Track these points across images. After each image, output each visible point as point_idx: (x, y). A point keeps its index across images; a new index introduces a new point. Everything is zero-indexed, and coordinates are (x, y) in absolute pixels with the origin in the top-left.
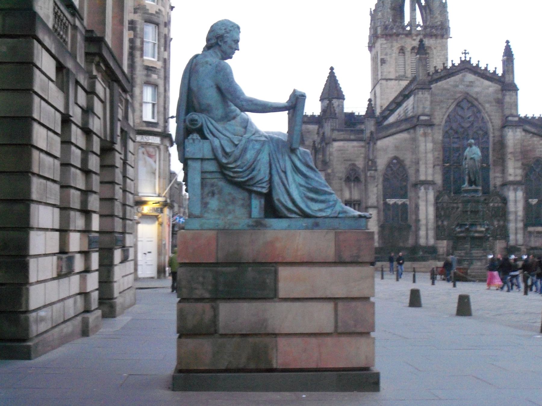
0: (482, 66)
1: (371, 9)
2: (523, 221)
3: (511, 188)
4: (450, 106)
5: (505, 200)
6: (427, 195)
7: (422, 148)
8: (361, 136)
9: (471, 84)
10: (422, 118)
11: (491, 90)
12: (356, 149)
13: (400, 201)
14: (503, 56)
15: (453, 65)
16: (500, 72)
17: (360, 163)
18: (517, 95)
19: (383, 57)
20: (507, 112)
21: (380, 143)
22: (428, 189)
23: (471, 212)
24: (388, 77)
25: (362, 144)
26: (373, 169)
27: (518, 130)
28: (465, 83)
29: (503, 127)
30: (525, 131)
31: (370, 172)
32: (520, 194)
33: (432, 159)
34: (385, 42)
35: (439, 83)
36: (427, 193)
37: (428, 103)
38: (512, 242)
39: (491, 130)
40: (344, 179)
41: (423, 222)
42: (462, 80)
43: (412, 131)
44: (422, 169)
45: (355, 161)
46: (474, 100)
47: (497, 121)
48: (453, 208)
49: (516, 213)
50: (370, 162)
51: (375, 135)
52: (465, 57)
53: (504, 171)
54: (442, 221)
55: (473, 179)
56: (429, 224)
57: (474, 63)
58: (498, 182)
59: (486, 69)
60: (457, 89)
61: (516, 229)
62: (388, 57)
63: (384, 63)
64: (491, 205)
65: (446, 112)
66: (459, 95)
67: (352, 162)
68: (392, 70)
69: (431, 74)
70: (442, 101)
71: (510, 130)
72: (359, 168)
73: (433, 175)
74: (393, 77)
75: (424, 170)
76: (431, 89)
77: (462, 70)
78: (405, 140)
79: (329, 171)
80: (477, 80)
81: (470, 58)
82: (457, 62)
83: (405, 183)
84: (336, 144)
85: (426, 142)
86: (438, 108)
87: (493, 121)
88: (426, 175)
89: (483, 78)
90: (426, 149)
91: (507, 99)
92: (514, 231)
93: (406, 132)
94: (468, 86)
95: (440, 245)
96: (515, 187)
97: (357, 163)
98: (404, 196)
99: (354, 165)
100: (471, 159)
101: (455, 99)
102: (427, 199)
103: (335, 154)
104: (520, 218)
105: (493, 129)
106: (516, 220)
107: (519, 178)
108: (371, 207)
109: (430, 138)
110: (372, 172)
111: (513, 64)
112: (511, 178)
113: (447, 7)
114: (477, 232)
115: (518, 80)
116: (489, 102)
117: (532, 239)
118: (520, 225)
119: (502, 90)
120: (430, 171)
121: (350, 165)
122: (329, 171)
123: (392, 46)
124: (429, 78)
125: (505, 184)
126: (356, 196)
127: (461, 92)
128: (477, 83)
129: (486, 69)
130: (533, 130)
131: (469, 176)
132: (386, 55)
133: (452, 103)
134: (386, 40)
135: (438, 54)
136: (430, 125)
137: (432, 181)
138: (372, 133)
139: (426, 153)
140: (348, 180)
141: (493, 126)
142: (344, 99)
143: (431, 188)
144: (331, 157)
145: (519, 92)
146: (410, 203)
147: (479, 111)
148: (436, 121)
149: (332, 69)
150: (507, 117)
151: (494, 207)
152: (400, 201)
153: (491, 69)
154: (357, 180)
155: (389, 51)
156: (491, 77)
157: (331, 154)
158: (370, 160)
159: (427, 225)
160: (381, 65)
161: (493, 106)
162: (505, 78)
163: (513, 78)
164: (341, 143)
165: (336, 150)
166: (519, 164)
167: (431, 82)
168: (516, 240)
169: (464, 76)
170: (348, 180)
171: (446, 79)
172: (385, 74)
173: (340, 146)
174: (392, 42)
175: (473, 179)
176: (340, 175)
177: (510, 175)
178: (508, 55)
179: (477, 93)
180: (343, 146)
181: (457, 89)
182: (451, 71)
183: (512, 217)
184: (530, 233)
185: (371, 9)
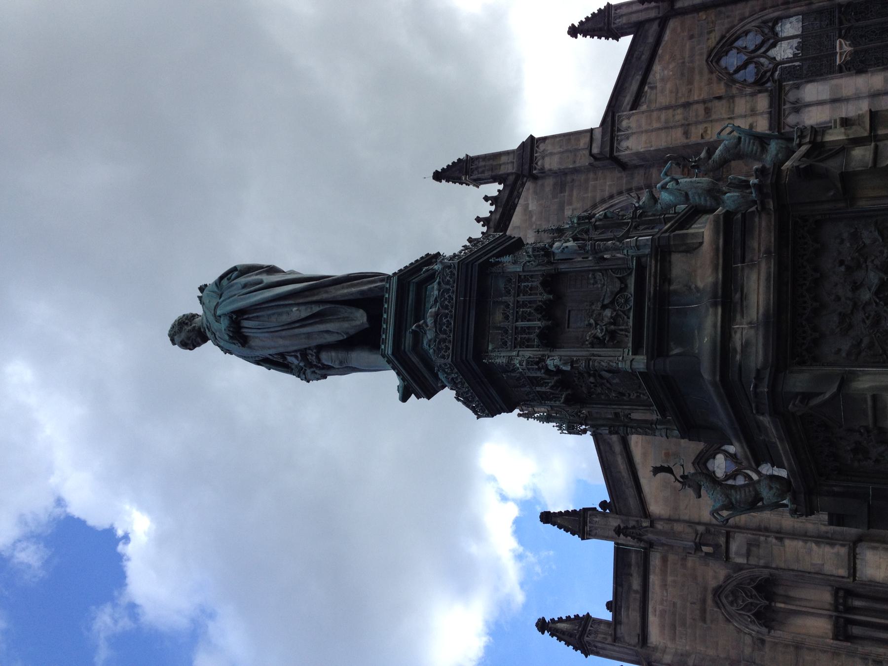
3: (792, 119)
8: (633, 558)
11: (533, 206)
12: (670, 579)
16: (493, 189)
17: (715, 574)
18: (544, 139)
20: (584, 160)
21: (656, 508)
23: (550, 339)
25: (655, 560)
26: (722, 541)
29: (623, 166)
30: (635, 105)
31: (732, 555)
40: (764, 630)
45: (705, 589)
47: (607, 183)
50: (705, 549)
55: (360, 318)
59: (486, 221)
67: (710, 601)
71: (624, 144)
72: (728, 577)
84: (655, 635)
87: (607, 194)
91: (551, 163)
97: (713, 584)
99: (717, 592)
107: (763, 102)
108: (853, 570)
110: (734, 547)
111: (478, 158)
116: (561, 208)
119: (535, 178)
121: (718, 604)
126: (826, 597)
129: (486, 221)
130: (634, 87)
140: (766, 617)
141: (620, 193)
145: (537, 136)
153: (486, 209)
156: (504, 206)
161: (571, 195)
162: (508, 174)
163: (507, 153)
164: (653, 621)
165: (673, 639)
166: (720, 109)
170: (766, 617)
173: (662, 627)
175: (360, 318)
176: (748, 640)
178: (462, 171)
180: (663, 613)
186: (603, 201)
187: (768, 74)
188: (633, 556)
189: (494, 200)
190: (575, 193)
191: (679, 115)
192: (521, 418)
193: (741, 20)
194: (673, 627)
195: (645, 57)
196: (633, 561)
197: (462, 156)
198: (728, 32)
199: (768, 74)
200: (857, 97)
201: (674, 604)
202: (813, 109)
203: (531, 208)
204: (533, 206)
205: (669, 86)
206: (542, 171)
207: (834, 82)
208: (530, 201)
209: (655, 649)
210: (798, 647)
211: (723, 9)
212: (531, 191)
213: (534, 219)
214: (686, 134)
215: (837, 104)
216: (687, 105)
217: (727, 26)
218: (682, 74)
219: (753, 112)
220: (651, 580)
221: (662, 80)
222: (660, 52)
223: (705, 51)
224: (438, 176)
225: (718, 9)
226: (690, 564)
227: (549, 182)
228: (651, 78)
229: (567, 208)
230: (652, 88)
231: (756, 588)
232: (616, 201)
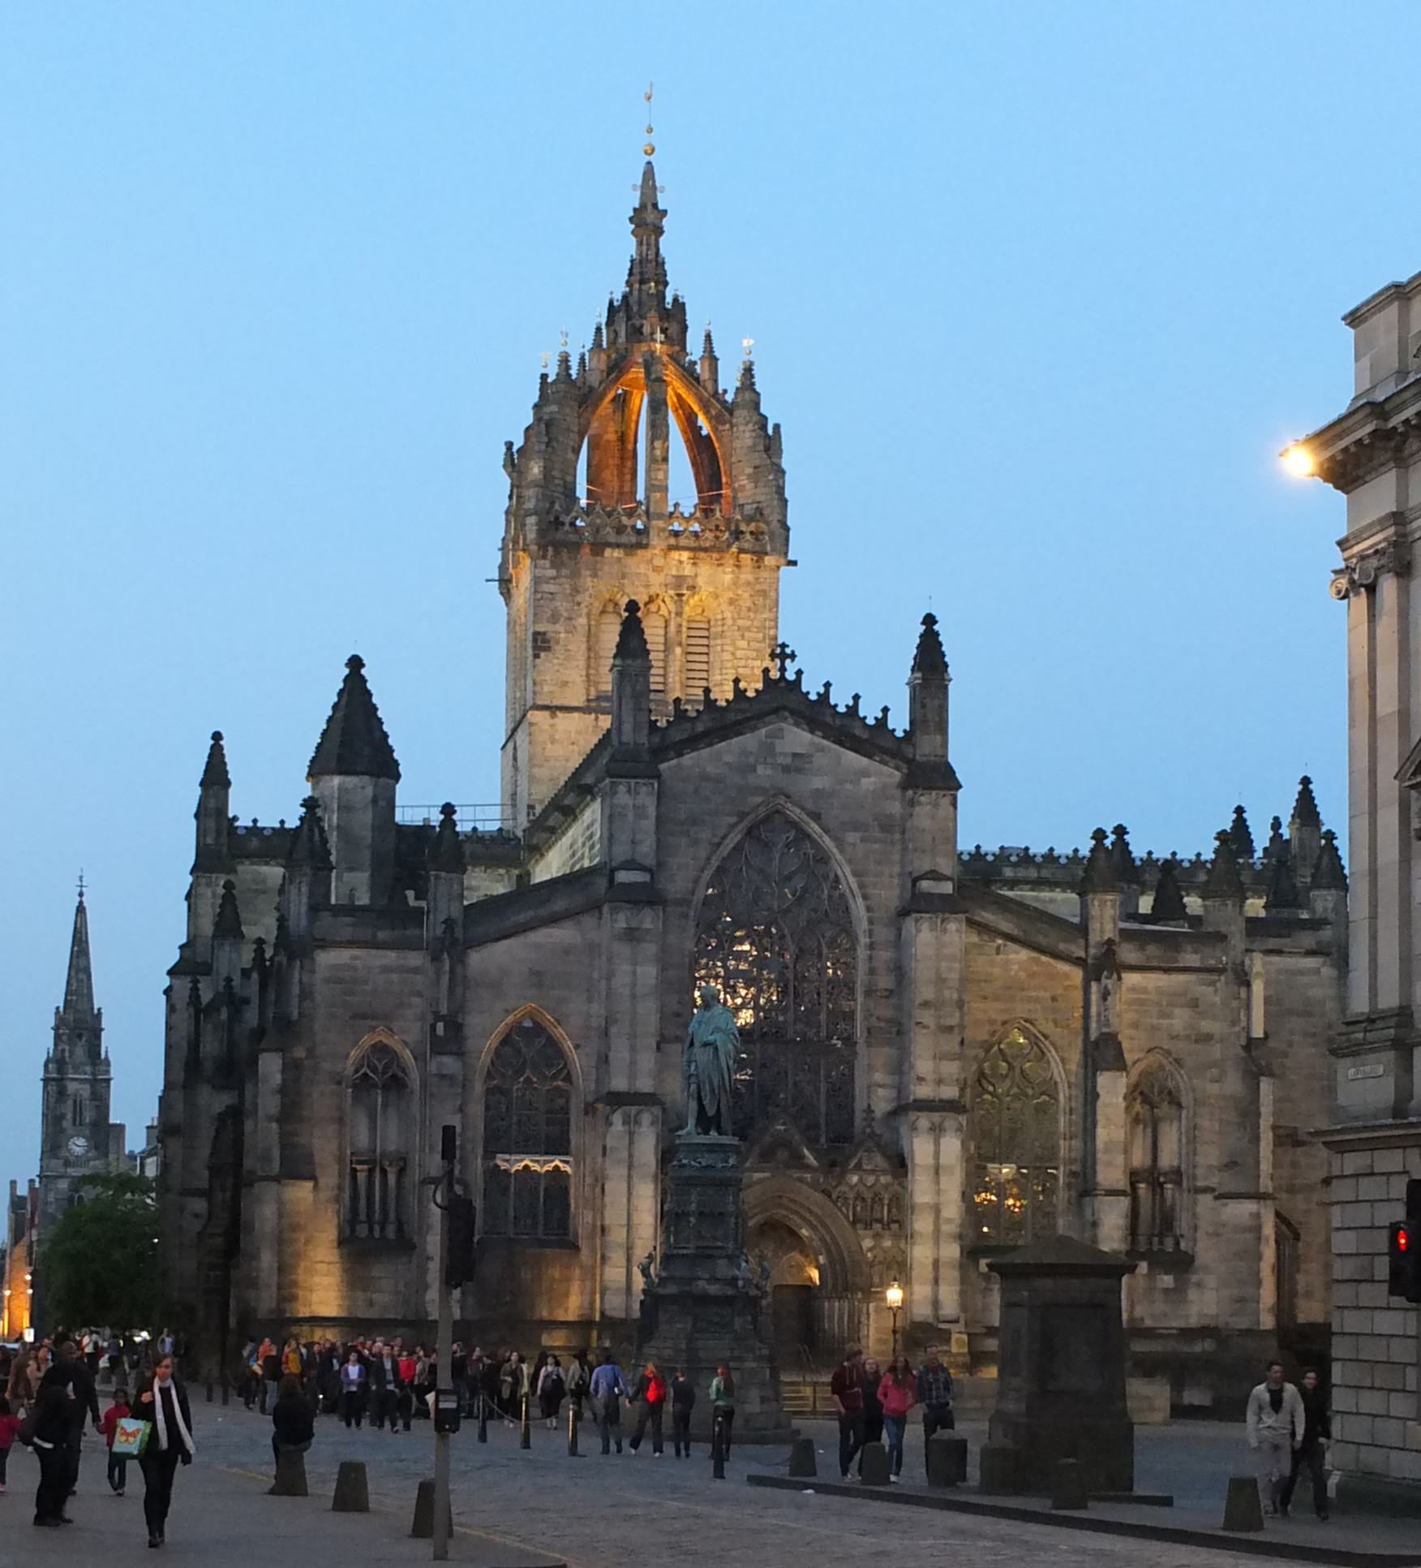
0: (840, 700)
1: (509, 445)
2: (961, 1237)
3: (924, 1121)
4: (724, 837)
5: (900, 1164)
6: (631, 1142)
7: (621, 982)
9: (799, 763)
10: (622, 877)
11: (867, 783)
12: (394, 977)
13: (540, 1165)
14: (913, 670)
15: (739, 693)
16: (899, 723)
18: (954, 805)
19: (541, 628)
21: (477, 959)
22: (637, 1123)
24: (556, 703)
25: (415, 959)
27: (952, 926)
28: (780, 760)
29: (904, 913)
32: (952, 1147)
33: (654, 1019)
34: (552, 572)
35: (688, 759)
36: (631, 1134)
37: (649, 824)
39: (865, 925)
41: (618, 1235)
42: (768, 750)
43: (588, 920)
44: (620, 1053)
46: (806, 818)
49: (937, 1210)
50: (440, 1026)
51: (459, 932)
52: (783, 669)
53: (900, 1068)
55: (711, 1112)
56: (639, 1243)
57: (812, 687)
58: (882, 1102)
61: (936, 1264)
62: (559, 627)
63: (548, 649)
64: (855, 1179)
65: (708, 859)
66: (759, 799)
68: (575, 674)
69: (662, 723)
70: (694, 821)
71: (925, 926)
73: (659, 1074)
74: (579, 701)
75: (626, 1055)
76: (658, 776)
77: (768, 714)
78: (567, 951)
79: (299, 1052)
80: (822, 749)
81: (799, 673)
82: (753, 686)
83: (561, 1101)
85: (635, 963)
86: (684, 841)
88: (632, 1076)
89: (841, 744)
90: (634, 985)
92: (928, 1273)
93: (569, 924)
94: (786, 769)
96: (936, 1117)
98: (558, 1145)
100: (706, 1044)
101: (742, 816)
102: (631, 1156)
103: (322, 991)
105: (871, 922)
107: (950, 1092)
109: (650, 949)
110: (447, 1060)
112: (923, 1091)
113: (779, 452)
114: (713, 1280)
115: (958, 757)
116: (856, 827)
118: (952, 1251)
119: (904, 786)
120: (647, 1060)
122: (299, 1052)
123: (576, 591)
124: (656, 739)
125: (903, 1108)
127: (758, 790)
128: (819, 760)
130: (1006, 926)
131: (700, 1099)
132: (554, 618)
133: (735, 825)
134: (553, 566)
135: (740, 622)
136: (648, 896)
137: (653, 1095)
138: (449, 923)
139: (633, 996)
140: (362, 1084)
141: (869, 909)
142: (397, 777)
144: (307, 1004)
145: (960, 793)
146: (577, 1165)
147: (823, 859)
148: (676, 884)
149: (355, 663)
150: (915, 881)
152: (540, 1165)
153: (869, 712)
154: (396, 1084)
155: (562, 606)
156: (872, 739)
157: (306, 994)
158: (438, 1017)
159: (629, 1249)
160: (536, 656)
163: (945, 744)
165: (328, 981)
166: (951, 1044)
167: (660, 752)
168: (936, 1303)
169: (778, 734)
171: (711, 745)
172: (546, 688)
173: (338, 967)
174: (575, 574)
175: (711, 1112)
177: (921, 1079)
179: (818, 794)
181: (751, 780)
182: (731, 717)
183: (922, 1224)
185: (509, 445)
186: (861, 886)
187: (991, 1088)
188: (417, 932)
189: (882, 722)
190: (876, 846)
191: (951, 995)
192: (504, 449)
193: (1063, 1060)
194: (340, 981)
195: (1041, 940)
196: (408, 933)
198: (1053, 1045)
199: (991, 1088)
200: (938, 1192)
201: (366, 983)
202: (932, 1147)
203: (864, 781)
204: (867, 783)
205: (997, 971)
206: (912, 803)
207: (958, 1169)
208: (877, 777)
209: (313, 960)
210: (341, 1120)
211: (1081, 1038)
212: (888, 780)
213: (849, 786)
214: (926, 1004)
215: (932, 1171)
216: (960, 1004)
217: (1059, 1043)
218: (1010, 988)
220: (389, 953)
221: (1007, 962)
222: (1044, 958)
223: (1033, 1016)
225: (1081, 1032)
226: (416, 1000)
227: (895, 808)
229: (858, 835)
230: (998, 949)
231: (394, 1076)
232: (860, 901)
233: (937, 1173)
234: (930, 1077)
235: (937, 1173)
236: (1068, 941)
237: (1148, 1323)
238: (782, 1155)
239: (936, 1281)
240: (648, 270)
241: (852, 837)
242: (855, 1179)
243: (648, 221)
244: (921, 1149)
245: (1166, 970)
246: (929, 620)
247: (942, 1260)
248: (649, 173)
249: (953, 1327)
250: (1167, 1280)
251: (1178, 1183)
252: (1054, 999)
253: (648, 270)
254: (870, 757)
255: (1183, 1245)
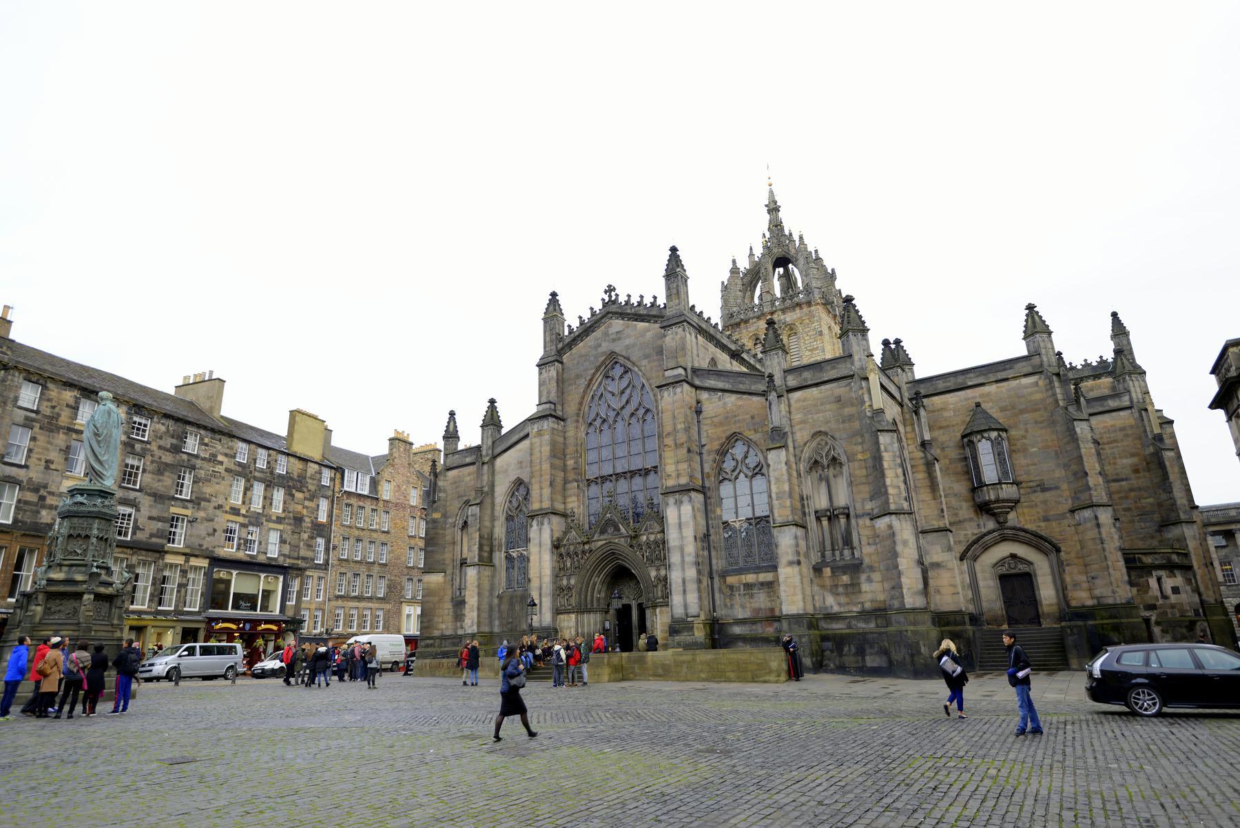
32: (687, 509)
38: (679, 611)
42: (606, 334)
48: (584, 552)
49: (682, 549)
52: (610, 296)
54: (569, 580)
60: (600, 350)
61: (684, 582)
64: (644, 538)
82: (598, 307)
89: (636, 320)
94: (614, 340)
95: (566, 624)
104: (690, 559)
106: (683, 561)
107: (684, 480)
116: (646, 357)
117: (737, 599)
118: (692, 573)
130: (720, 385)
143: (546, 521)
151: (648, 544)
153: (648, 301)
168: (686, 606)
179: (627, 347)
181: (600, 350)
183: (675, 558)
184: (731, 588)
195: (742, 387)
197: (664, 273)
219: (678, 476)
224: (674, 250)
228: (727, 394)
230: (720, 399)
233: (680, 525)
234: (674, 475)
235: (680, 525)
236: (756, 383)
237: (836, 609)
238: (611, 530)
239: (684, 591)
240: (776, 226)
241: (644, 362)
242: (644, 538)
243: (773, 209)
244: (671, 514)
245: (817, 385)
246: (674, 250)
247: (687, 579)
248: (771, 192)
249: (697, 621)
250: (845, 579)
251: (848, 516)
252: (753, 417)
253: (776, 226)
254: (649, 322)
255: (857, 554)
